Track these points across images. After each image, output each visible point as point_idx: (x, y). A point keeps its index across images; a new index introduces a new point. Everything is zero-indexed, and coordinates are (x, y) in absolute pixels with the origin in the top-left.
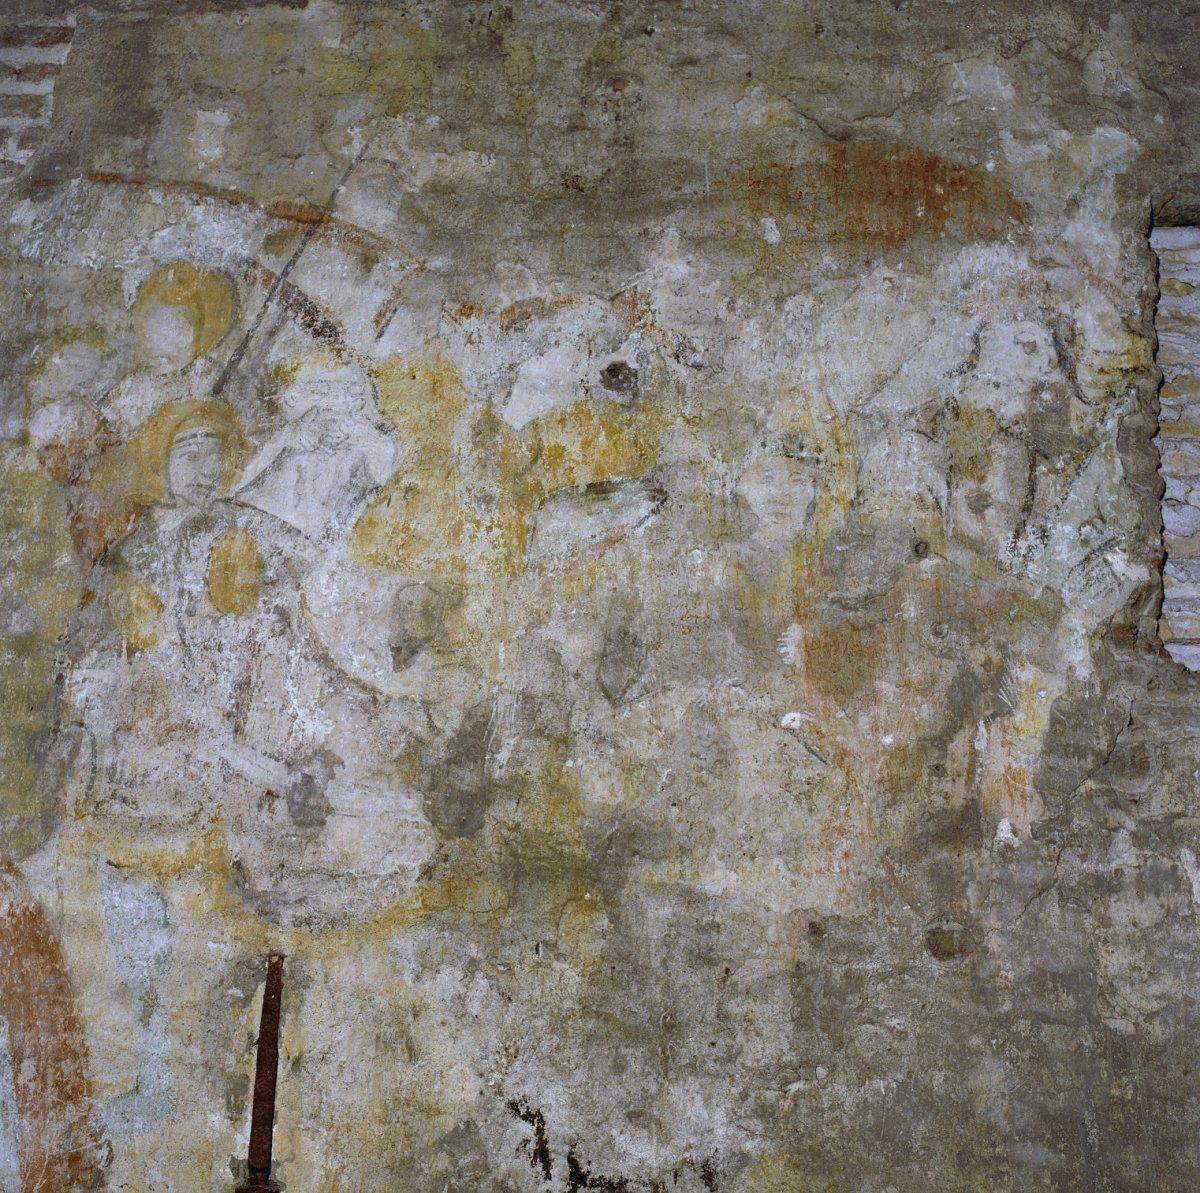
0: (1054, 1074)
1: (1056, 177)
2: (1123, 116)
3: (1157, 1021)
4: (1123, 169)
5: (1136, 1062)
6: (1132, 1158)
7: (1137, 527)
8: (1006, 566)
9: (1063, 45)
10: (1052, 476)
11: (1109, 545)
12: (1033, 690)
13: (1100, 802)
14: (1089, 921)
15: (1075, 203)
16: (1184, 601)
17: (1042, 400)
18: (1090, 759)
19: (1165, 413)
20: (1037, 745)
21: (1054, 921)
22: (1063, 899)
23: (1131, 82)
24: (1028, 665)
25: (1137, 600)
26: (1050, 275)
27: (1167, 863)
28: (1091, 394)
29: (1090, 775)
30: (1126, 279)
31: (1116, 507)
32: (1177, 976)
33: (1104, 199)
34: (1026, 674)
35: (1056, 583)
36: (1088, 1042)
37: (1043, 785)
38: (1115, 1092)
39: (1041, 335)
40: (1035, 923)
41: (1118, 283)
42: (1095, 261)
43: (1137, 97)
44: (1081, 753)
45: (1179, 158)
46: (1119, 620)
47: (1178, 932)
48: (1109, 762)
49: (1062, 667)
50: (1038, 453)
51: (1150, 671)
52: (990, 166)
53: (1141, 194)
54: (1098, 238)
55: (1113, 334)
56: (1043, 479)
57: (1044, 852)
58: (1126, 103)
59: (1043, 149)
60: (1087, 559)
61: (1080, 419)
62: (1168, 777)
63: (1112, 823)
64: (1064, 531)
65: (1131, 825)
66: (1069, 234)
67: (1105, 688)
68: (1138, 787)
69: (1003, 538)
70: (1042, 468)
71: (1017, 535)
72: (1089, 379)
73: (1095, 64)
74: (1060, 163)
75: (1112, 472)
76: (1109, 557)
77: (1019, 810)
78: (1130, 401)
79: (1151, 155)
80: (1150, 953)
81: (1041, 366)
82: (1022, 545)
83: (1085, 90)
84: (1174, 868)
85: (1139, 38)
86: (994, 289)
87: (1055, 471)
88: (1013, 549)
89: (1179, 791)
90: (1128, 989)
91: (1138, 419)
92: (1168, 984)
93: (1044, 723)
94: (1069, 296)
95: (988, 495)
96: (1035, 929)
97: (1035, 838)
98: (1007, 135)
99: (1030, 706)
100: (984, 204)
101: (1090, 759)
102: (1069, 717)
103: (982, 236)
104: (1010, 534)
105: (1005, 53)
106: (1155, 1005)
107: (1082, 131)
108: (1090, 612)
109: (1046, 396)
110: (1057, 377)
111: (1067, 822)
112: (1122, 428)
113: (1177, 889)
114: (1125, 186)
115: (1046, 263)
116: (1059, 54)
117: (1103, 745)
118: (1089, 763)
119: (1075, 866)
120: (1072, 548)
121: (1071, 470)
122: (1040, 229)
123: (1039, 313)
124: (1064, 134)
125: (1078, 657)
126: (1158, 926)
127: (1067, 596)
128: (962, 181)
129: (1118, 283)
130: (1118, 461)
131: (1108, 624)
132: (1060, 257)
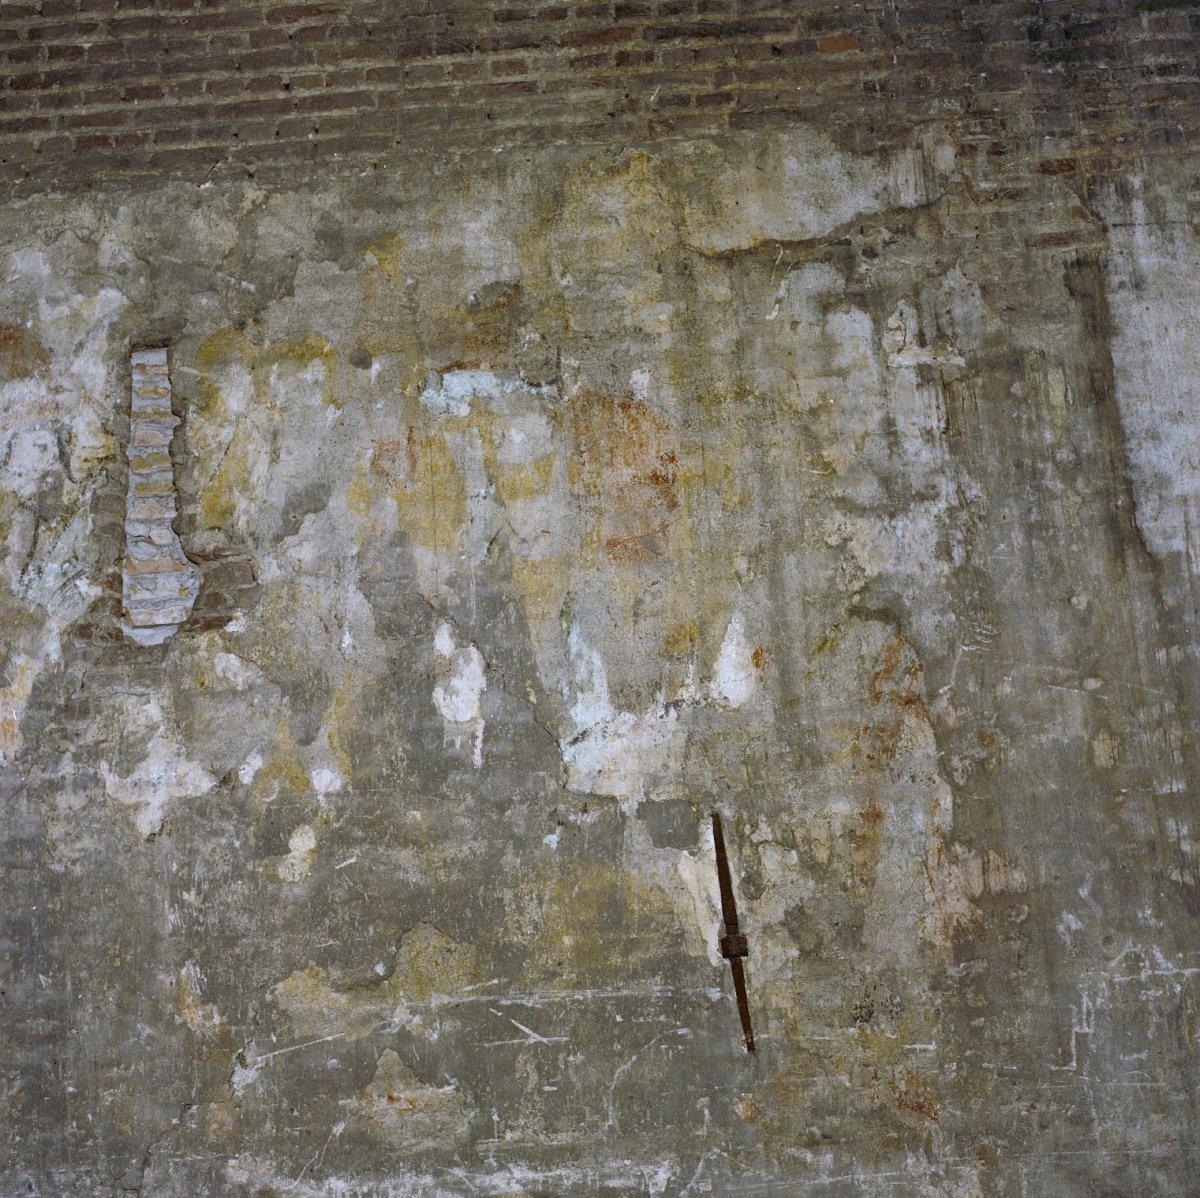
0: (16, 899)
1: (70, 328)
2: (119, 280)
3: (78, 864)
4: (115, 319)
5: (64, 888)
6: (56, 943)
7: (97, 562)
8: (15, 593)
9: (86, 232)
10: (48, 533)
11: (78, 575)
12: (23, 670)
13: (56, 736)
14: (44, 808)
15: (81, 345)
16: (140, 602)
17: (47, 483)
18: (53, 710)
19: (134, 480)
20: (23, 704)
21: (24, 809)
22: (29, 796)
23: (127, 255)
24: (22, 654)
25: (94, 607)
26: (60, 398)
27: (91, 771)
28: (77, 476)
29: (53, 720)
30: (107, 396)
31: (86, 550)
32: (92, 837)
33: (100, 342)
34: (20, 660)
35: (44, 601)
36: (37, 878)
37: (25, 727)
38: (50, 906)
39: (49, 438)
40: (12, 811)
41: (101, 399)
42: (89, 385)
43: (130, 265)
44: (48, 707)
45: (151, 308)
46: (81, 622)
47: (95, 812)
48: (68, 710)
49: (42, 654)
50: (41, 518)
51: (98, 653)
52: (29, 324)
53: (123, 337)
54: (92, 370)
55: (96, 435)
56: (42, 535)
57: (21, 768)
58: (122, 271)
59: (64, 310)
60: (65, 585)
61: (69, 493)
62: (98, 718)
63: (62, 749)
64: (53, 567)
65: (73, 749)
66: (75, 369)
67: (66, 666)
68: (81, 725)
69: (15, 575)
70: (43, 528)
71: (23, 573)
72: (77, 466)
73: (105, 245)
74: (76, 316)
75: (86, 527)
76: (78, 582)
77: (9, 743)
78: (101, 480)
79: (135, 307)
80: (78, 824)
81: (48, 461)
82: (26, 579)
83: (96, 264)
84: (96, 773)
85: (137, 222)
86: (22, 410)
87: (49, 529)
88: (21, 581)
89: (105, 726)
90: (63, 846)
91: (107, 490)
92: (87, 842)
93: (28, 689)
94: (69, 411)
95: (8, 548)
96: (12, 814)
97: (16, 759)
98: (42, 301)
99: (21, 680)
100: (23, 352)
101: (53, 710)
102: (43, 684)
103: (18, 375)
104: (19, 572)
105: (49, 240)
106: (77, 855)
107: (91, 294)
108: (63, 618)
109: (49, 480)
110: (58, 466)
111: (38, 748)
112: (96, 498)
113: (97, 785)
114: (115, 333)
115: (58, 390)
116: (82, 240)
117: (62, 701)
118: (52, 713)
119: (37, 776)
120: (56, 578)
121: (60, 527)
122: (55, 368)
123: (50, 424)
124: (80, 298)
125: (53, 647)
126: (84, 808)
127: (50, 609)
128: (10, 337)
129: (101, 399)
130: (90, 520)
131: (72, 626)
132: (66, 383)
